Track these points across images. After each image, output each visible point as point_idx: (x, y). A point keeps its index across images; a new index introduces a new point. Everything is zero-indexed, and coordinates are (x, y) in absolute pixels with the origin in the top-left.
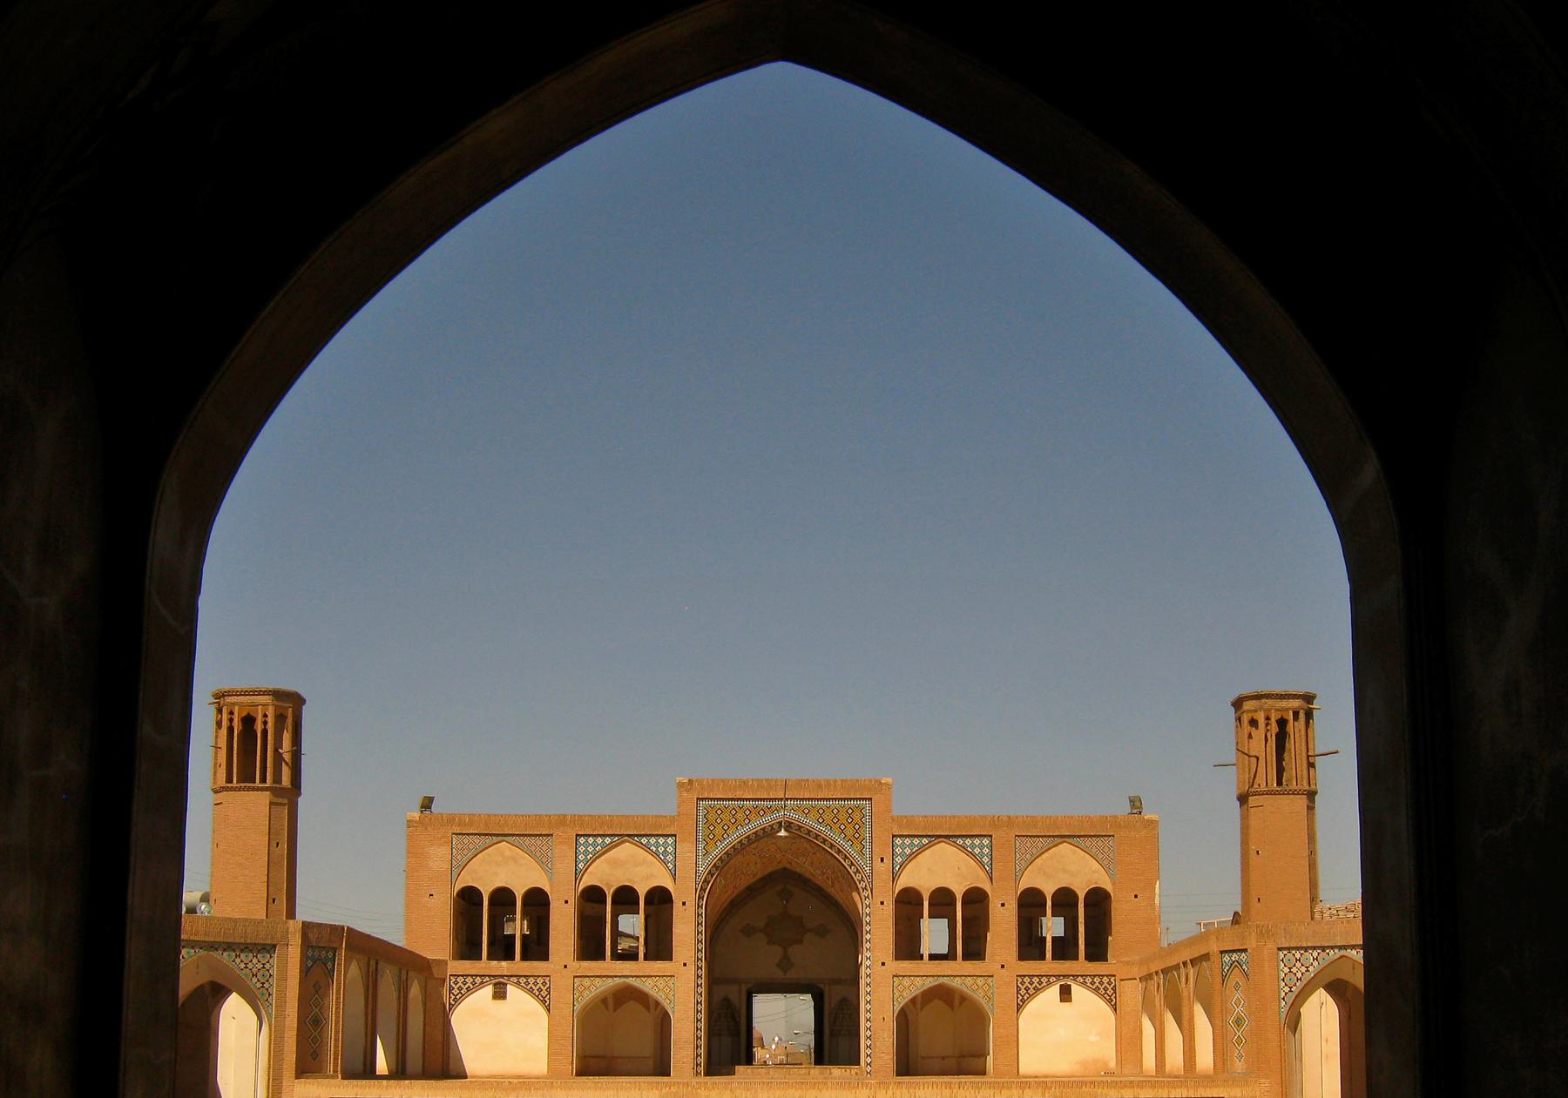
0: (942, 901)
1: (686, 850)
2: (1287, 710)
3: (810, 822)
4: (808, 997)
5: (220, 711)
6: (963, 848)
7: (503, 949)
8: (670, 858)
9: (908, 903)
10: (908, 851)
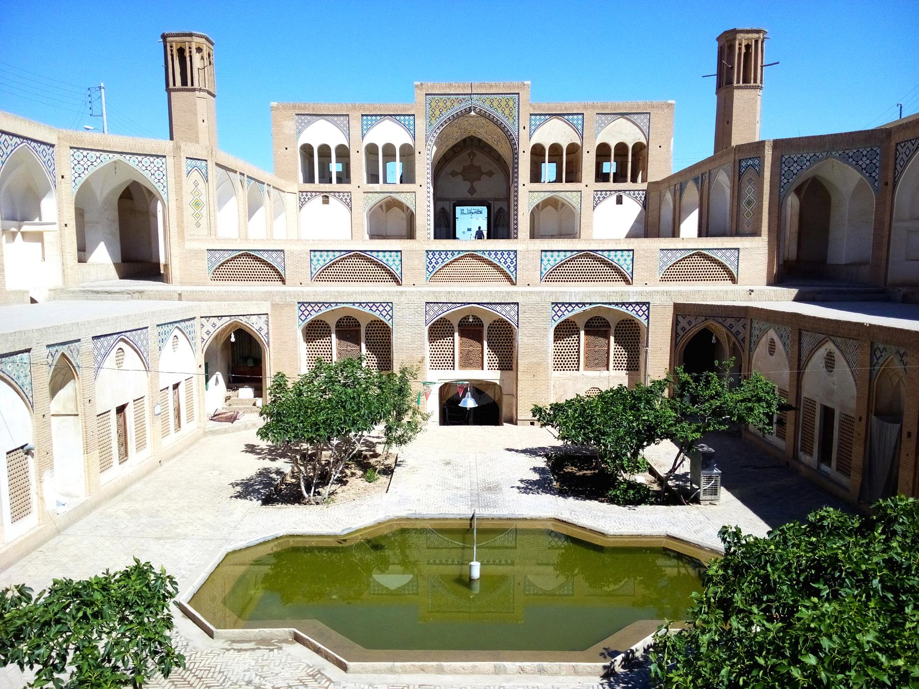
0: (556, 149)
1: (421, 124)
2: (751, 39)
3: (486, 107)
4: (484, 209)
5: (165, 47)
6: (567, 122)
7: (326, 177)
8: (412, 127)
9: (537, 152)
10: (538, 123)
